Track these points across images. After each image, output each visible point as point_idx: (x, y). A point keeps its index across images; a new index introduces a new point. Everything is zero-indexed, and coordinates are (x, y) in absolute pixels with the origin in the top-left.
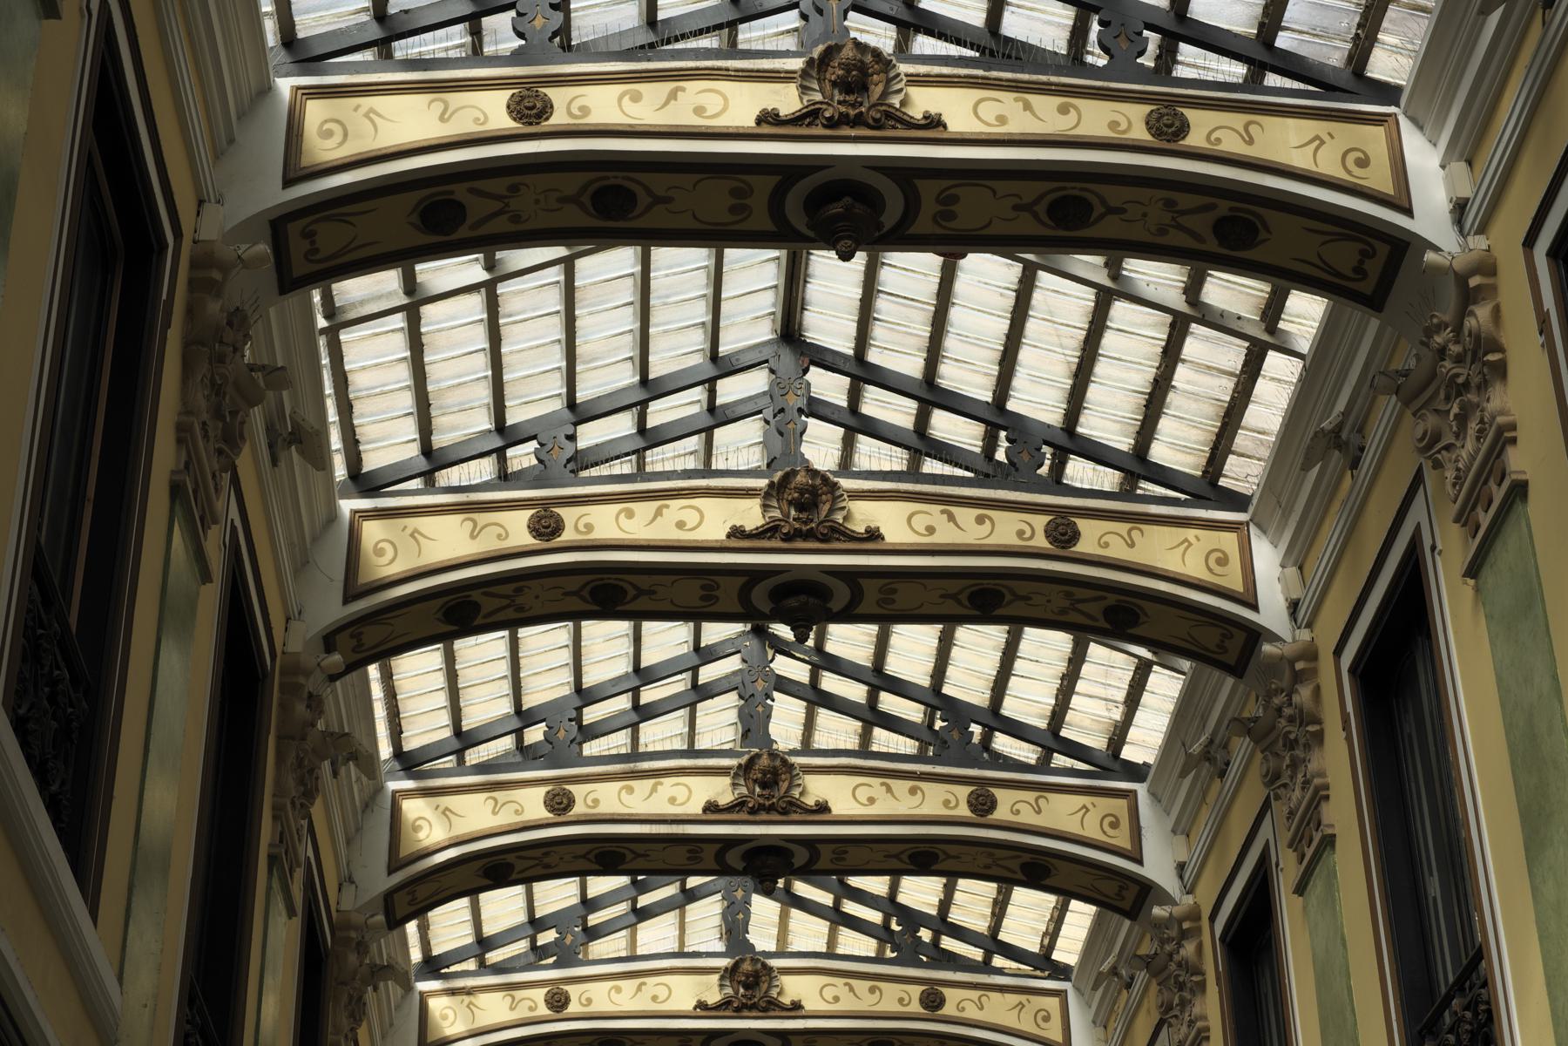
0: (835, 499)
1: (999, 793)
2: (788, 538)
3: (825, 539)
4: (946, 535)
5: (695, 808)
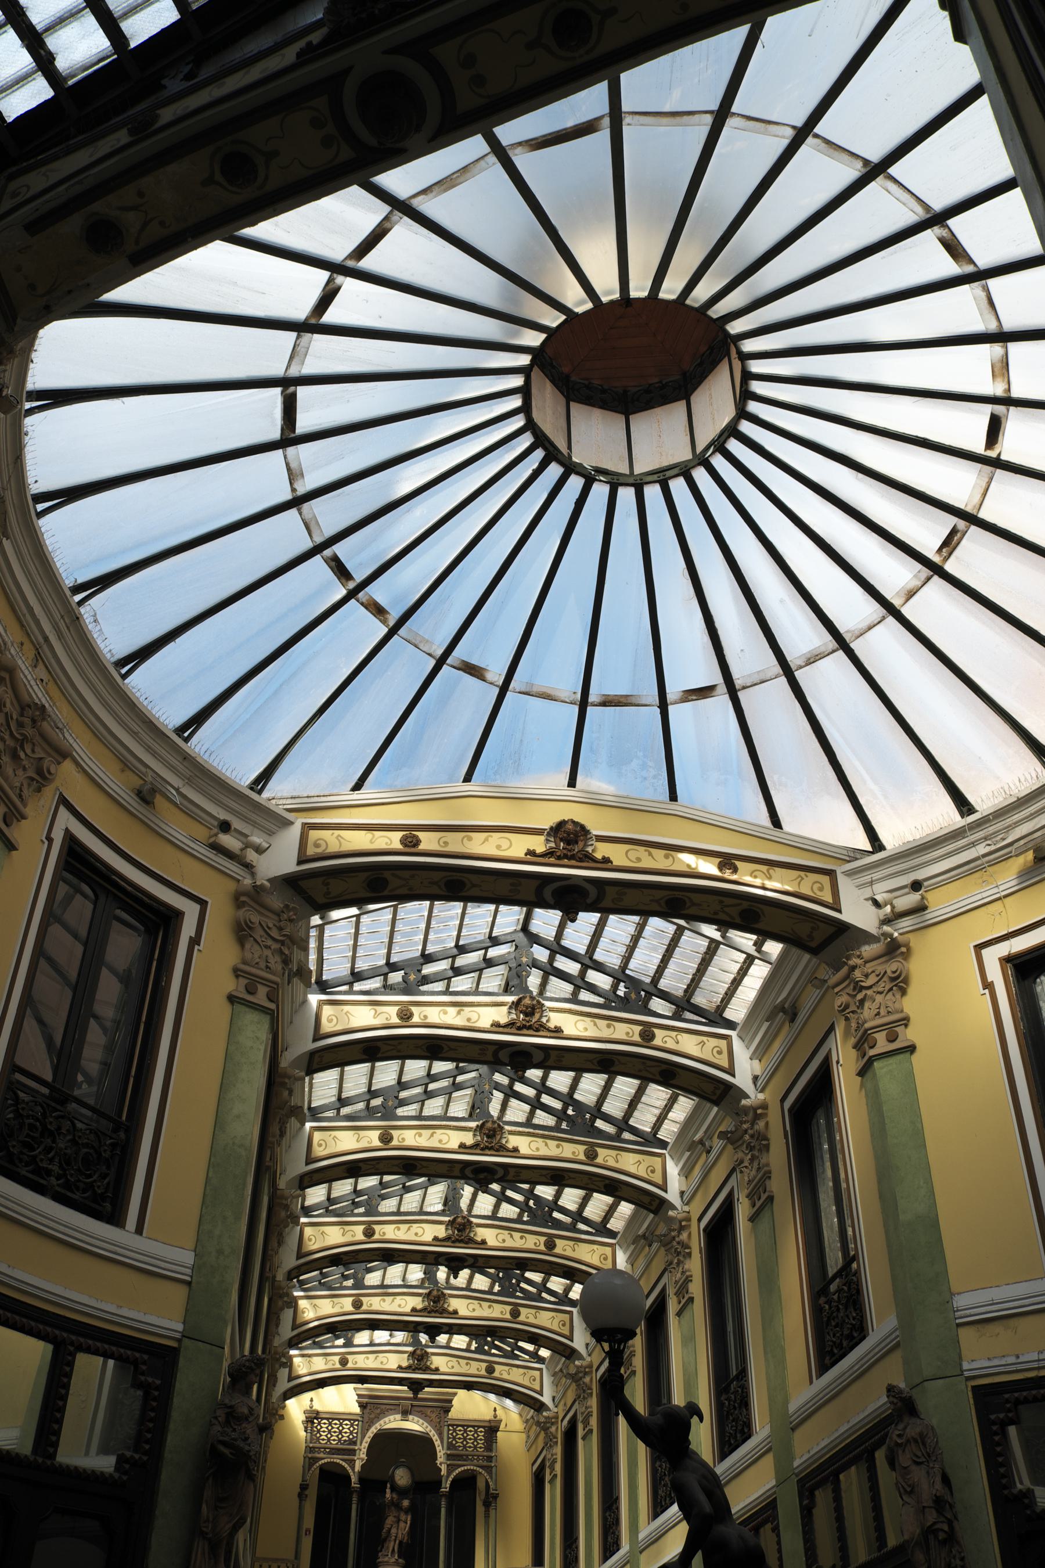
0: (471, 1227)
1: (522, 1309)
2: (453, 1242)
3: (467, 1243)
4: (509, 1243)
5: (408, 1309)
